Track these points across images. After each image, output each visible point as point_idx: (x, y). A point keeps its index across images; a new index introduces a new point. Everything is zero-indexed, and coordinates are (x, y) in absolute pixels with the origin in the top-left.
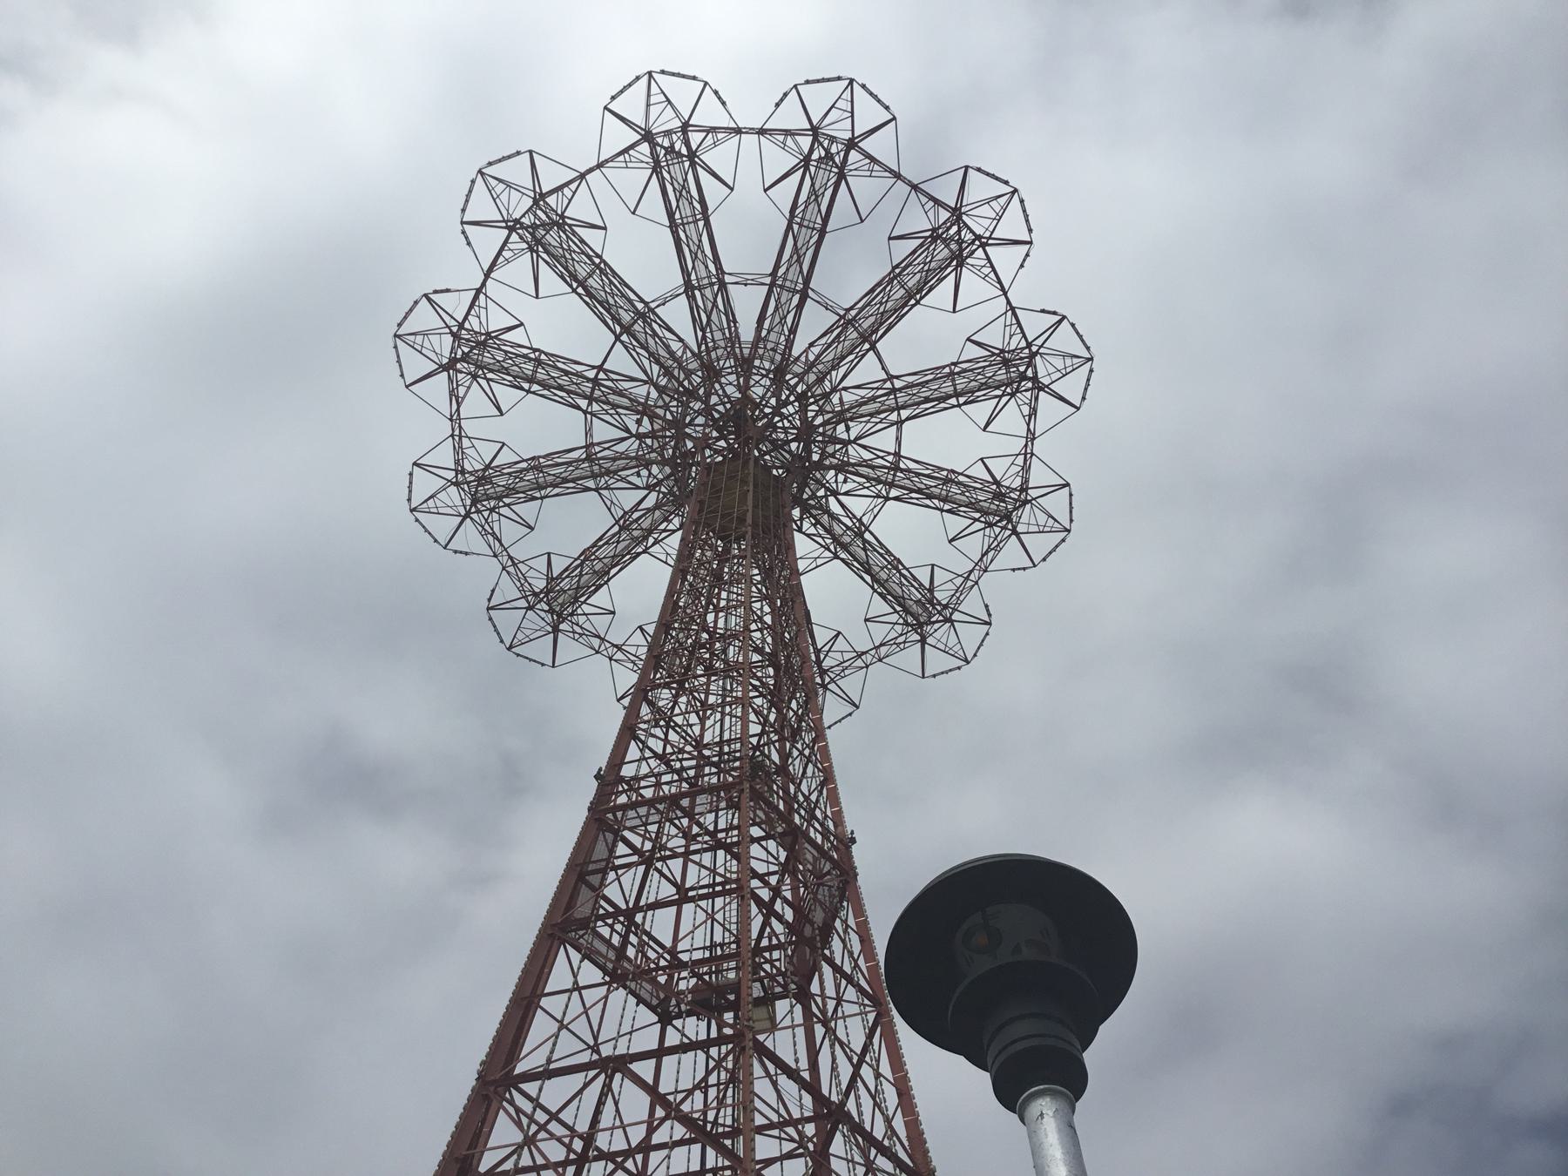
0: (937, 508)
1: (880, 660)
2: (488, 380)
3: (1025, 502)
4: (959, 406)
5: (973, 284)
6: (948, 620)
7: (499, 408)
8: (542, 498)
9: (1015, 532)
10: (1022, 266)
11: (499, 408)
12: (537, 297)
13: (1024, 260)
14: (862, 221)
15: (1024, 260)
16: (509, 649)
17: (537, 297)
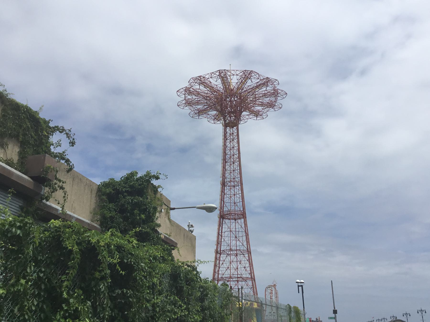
1: (250, 118)
16: (192, 117)
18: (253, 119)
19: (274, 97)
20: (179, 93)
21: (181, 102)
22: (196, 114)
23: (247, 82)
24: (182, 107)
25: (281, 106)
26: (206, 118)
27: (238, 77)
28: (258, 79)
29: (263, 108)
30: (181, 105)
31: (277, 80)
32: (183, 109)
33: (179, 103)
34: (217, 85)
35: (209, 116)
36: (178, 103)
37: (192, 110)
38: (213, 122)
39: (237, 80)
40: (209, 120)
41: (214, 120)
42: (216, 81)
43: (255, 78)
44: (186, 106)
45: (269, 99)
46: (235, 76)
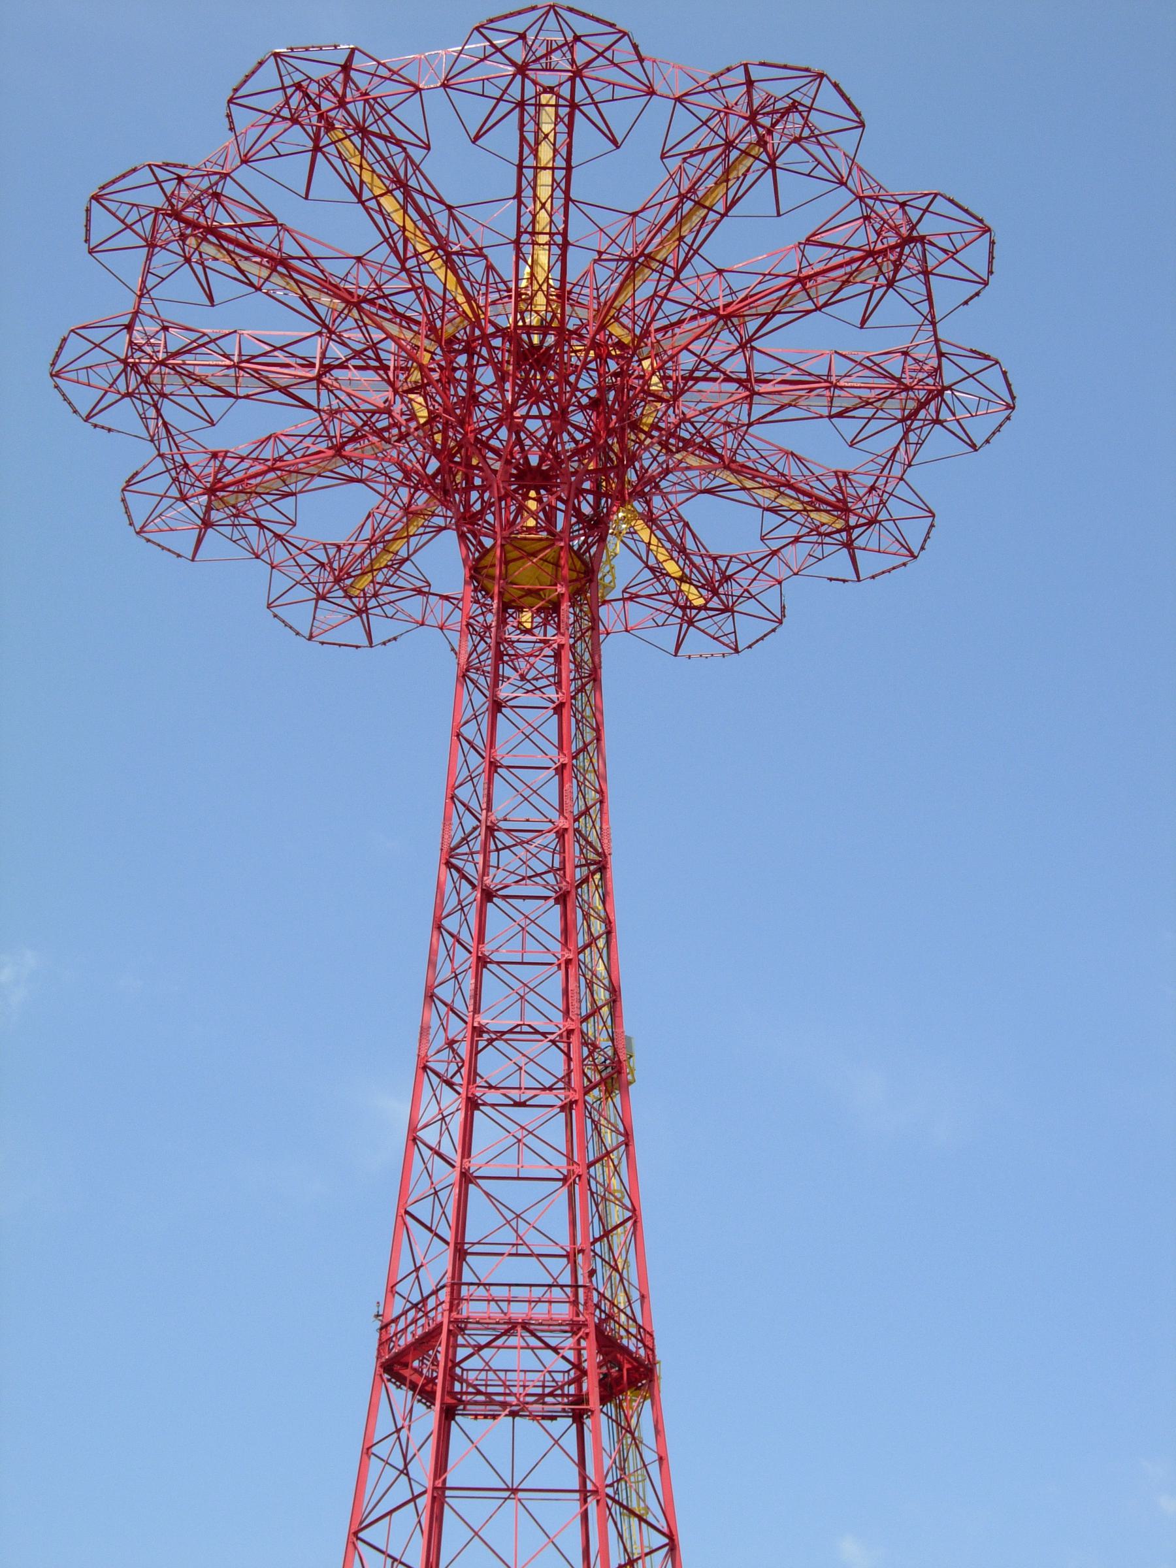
0: (759, 506)
1: (627, 631)
2: (204, 268)
3: (872, 522)
4: (830, 417)
5: (892, 308)
6: (727, 609)
7: (211, 298)
8: (237, 397)
9: (849, 545)
10: (966, 303)
11: (211, 298)
12: (306, 198)
13: (971, 298)
14: (779, 215)
15: (971, 298)
17: (306, 198)
18: (652, 634)
19: (900, 421)
20: (103, 224)
21: (97, 335)
22: (184, 498)
23: (734, 203)
24: (85, 399)
25: (914, 533)
26: (258, 557)
27: (684, 122)
28: (842, 183)
29: (772, 520)
30: (83, 376)
31: (987, 230)
32: (87, 418)
33: (76, 346)
34: (450, 208)
35: (279, 553)
36: (65, 340)
37: (165, 449)
38: (300, 615)
39: (663, 156)
40: (281, 582)
41: (323, 597)
42: (477, 137)
43: (819, 163)
44: (129, 395)
45: (849, 427)
46: (660, 107)
